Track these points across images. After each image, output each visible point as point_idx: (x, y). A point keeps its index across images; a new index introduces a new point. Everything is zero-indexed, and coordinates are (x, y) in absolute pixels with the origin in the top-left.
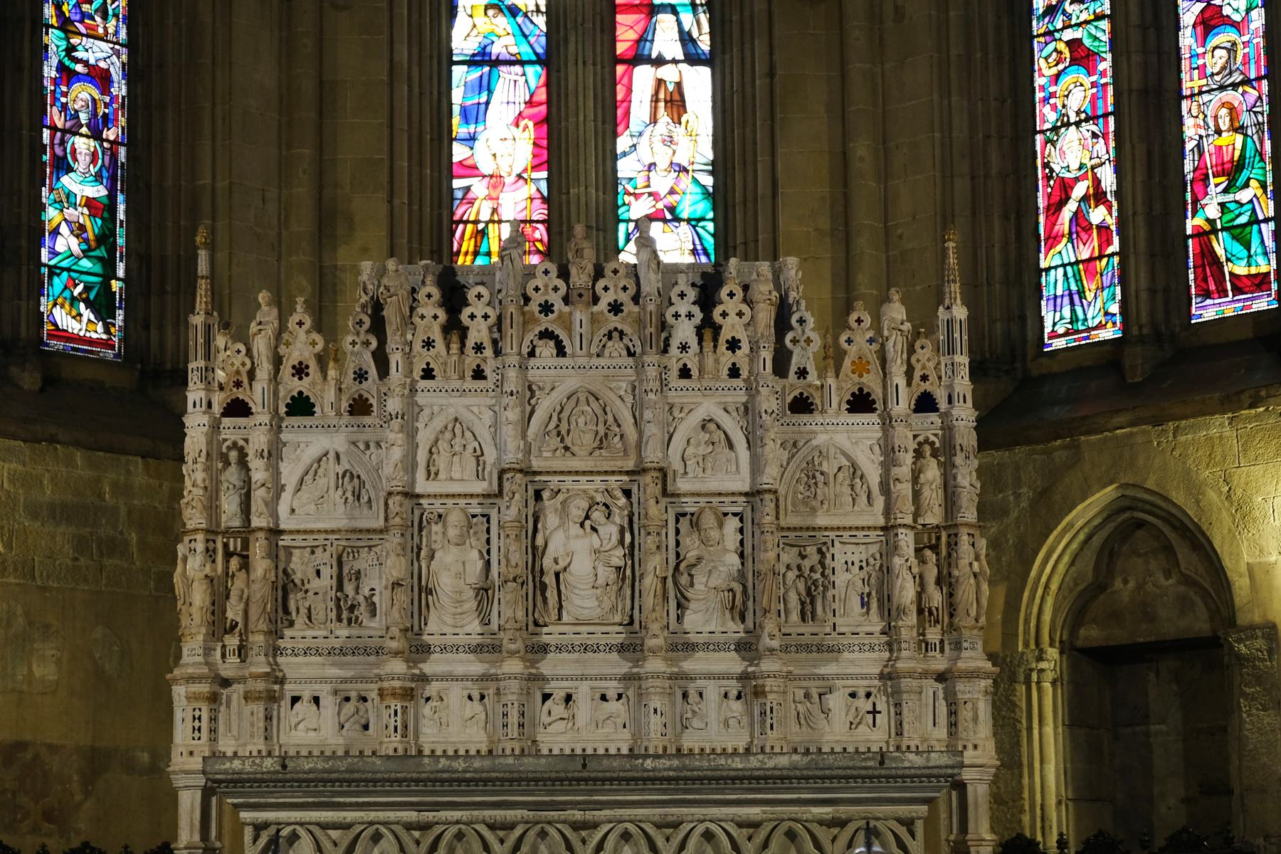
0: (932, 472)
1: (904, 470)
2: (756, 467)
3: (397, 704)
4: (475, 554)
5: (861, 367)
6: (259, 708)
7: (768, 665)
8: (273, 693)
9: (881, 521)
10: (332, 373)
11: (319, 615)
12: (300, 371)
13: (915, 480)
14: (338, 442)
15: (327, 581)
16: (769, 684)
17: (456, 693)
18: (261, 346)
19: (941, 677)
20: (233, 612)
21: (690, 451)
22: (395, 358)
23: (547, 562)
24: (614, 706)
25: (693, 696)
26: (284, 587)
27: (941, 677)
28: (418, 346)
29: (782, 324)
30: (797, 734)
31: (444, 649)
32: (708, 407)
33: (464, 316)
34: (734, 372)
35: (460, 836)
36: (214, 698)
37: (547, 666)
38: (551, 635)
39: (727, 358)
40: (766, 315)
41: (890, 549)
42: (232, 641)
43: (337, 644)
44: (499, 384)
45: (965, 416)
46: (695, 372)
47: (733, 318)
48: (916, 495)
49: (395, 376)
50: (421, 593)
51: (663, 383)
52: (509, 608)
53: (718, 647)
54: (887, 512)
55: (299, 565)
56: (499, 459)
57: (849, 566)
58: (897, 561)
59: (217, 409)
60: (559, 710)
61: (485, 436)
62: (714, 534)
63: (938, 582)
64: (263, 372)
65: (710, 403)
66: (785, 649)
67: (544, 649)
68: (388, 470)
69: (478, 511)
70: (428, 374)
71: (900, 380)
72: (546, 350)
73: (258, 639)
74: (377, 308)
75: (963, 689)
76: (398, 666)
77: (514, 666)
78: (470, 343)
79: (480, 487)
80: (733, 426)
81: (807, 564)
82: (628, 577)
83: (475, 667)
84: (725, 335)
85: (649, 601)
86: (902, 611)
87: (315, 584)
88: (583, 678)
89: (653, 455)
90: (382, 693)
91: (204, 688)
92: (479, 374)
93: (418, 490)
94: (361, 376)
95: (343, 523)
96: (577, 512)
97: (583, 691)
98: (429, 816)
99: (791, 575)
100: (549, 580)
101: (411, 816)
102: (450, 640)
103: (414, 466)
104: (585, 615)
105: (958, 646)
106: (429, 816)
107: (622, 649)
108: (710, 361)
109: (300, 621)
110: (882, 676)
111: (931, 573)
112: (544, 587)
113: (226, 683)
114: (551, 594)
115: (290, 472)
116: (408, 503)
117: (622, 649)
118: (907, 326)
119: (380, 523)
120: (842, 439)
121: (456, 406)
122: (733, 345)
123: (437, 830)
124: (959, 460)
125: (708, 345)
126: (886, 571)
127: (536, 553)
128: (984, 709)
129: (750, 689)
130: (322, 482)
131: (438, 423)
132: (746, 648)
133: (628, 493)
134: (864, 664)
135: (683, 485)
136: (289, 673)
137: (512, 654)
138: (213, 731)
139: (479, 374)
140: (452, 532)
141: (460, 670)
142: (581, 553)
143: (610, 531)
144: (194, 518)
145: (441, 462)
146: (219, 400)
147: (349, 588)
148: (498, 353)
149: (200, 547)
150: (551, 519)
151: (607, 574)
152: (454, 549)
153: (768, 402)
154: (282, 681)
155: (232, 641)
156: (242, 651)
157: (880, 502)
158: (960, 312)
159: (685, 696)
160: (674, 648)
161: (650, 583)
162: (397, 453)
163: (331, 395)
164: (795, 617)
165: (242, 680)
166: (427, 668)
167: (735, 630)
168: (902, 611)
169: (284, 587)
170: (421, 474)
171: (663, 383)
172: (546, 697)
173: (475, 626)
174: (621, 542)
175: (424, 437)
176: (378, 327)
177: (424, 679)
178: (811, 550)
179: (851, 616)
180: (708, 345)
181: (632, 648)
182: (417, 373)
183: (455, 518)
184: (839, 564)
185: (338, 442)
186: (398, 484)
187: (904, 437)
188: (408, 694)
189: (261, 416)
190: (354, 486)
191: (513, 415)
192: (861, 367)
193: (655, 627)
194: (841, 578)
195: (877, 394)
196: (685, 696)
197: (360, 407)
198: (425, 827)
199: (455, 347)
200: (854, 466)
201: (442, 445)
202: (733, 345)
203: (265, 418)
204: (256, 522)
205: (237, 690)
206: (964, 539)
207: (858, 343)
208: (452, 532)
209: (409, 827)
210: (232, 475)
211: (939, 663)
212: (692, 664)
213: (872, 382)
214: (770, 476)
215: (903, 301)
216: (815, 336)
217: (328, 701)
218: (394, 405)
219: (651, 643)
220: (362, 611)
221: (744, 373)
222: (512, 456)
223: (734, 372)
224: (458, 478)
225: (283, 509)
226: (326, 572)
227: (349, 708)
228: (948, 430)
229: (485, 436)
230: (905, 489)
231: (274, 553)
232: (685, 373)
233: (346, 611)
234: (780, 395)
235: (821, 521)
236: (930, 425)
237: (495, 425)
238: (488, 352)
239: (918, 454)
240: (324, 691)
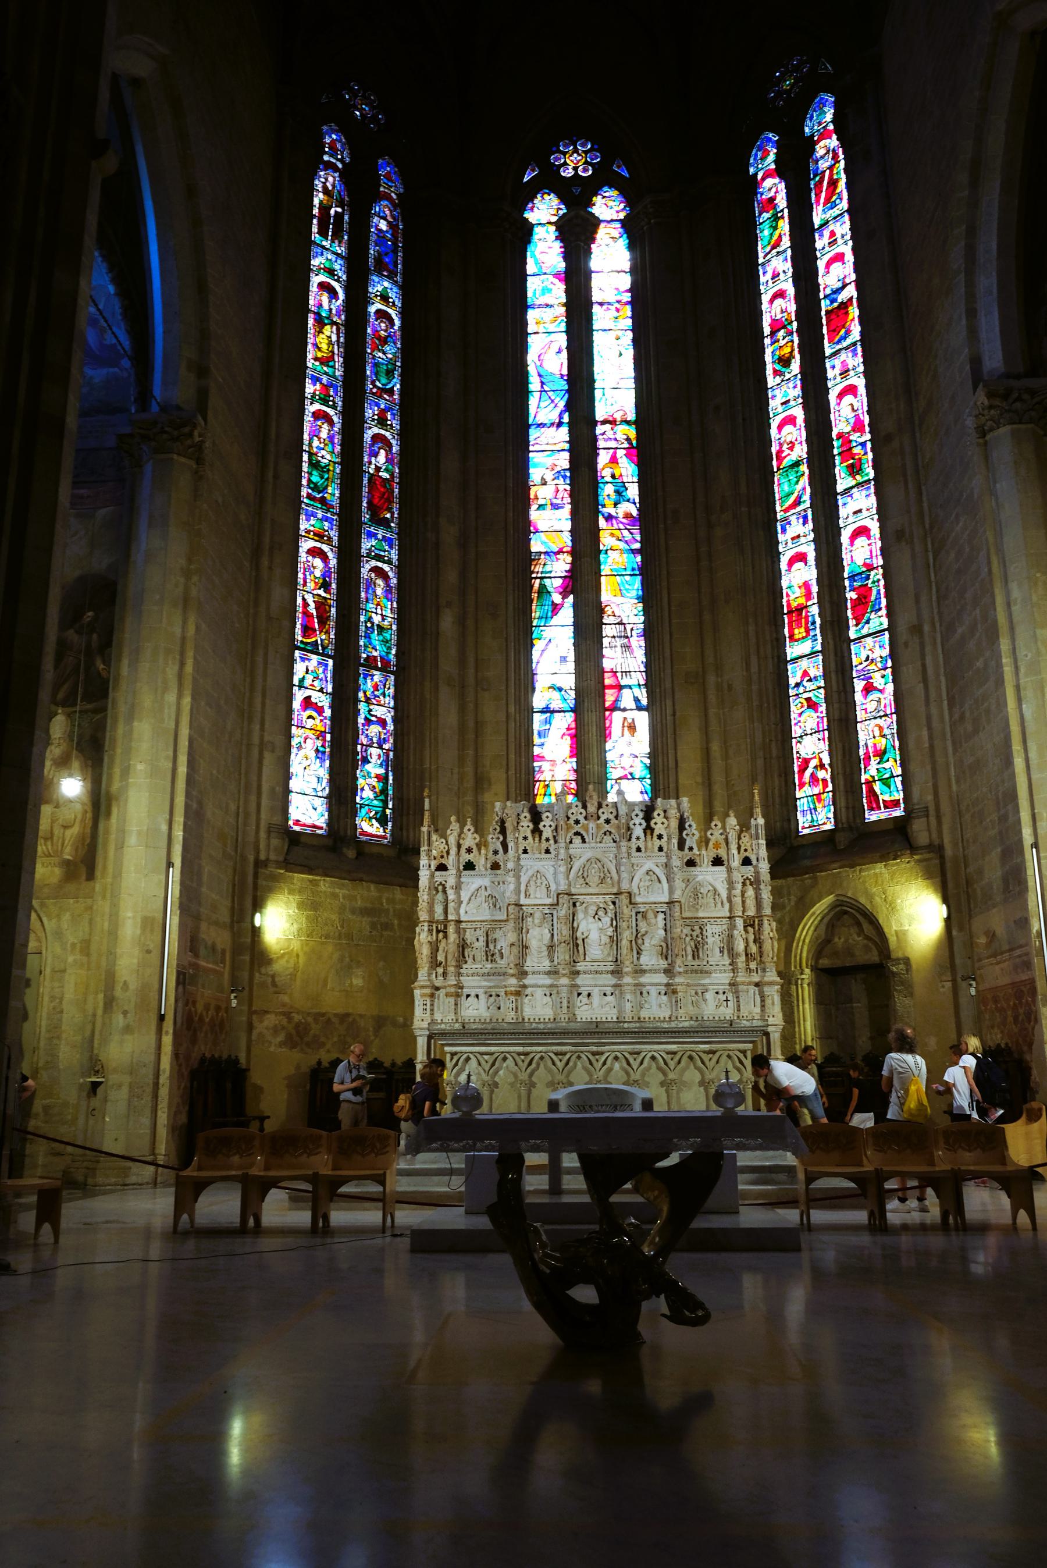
0: (750, 892)
1: (738, 892)
2: (671, 891)
3: (513, 998)
4: (547, 931)
5: (717, 846)
6: (452, 1000)
7: (678, 980)
8: (458, 994)
9: (728, 915)
10: (483, 851)
11: (478, 958)
12: (469, 851)
13: (743, 895)
14: (486, 882)
15: (481, 943)
16: (679, 988)
17: (539, 993)
18: (452, 840)
19: (757, 985)
20: (440, 957)
21: (642, 884)
22: (511, 845)
23: (579, 934)
24: (609, 998)
25: (645, 994)
26: (463, 946)
27: (757, 985)
28: (521, 839)
29: (681, 827)
30: (692, 1011)
31: (533, 973)
32: (649, 865)
33: (541, 826)
34: (661, 849)
35: (542, 1058)
36: (432, 996)
37: (579, 981)
38: (581, 966)
39: (657, 843)
40: (674, 824)
41: (732, 927)
42: (440, 970)
43: (486, 971)
44: (557, 856)
45: (764, 867)
46: (643, 849)
47: (659, 825)
48: (743, 902)
49: (511, 852)
50: (524, 947)
51: (629, 854)
52: (562, 954)
53: (656, 972)
54: (731, 910)
55: (469, 936)
56: (557, 889)
57: (714, 936)
58: (736, 932)
59: (433, 868)
60: (585, 1000)
61: (551, 878)
62: (653, 921)
63: (755, 941)
64: (453, 851)
65: (651, 863)
66: (686, 972)
67: (578, 973)
68: (508, 894)
69: (548, 911)
70: (525, 851)
71: (735, 852)
72: (577, 840)
73: (451, 969)
74: (502, 822)
75: (767, 990)
76: (513, 981)
77: (565, 981)
78: (544, 837)
79: (549, 901)
80: (660, 872)
81: (694, 934)
82: (615, 940)
83: (548, 981)
84: (656, 833)
85: (624, 951)
86: (738, 955)
87: (476, 944)
88: (596, 986)
89: (625, 886)
90: (506, 993)
91: (428, 991)
92: (547, 851)
93: (522, 903)
94: (496, 852)
95: (488, 918)
96: (592, 912)
97: (596, 992)
98: (528, 1049)
99: (688, 939)
100: (580, 942)
101: (520, 1049)
102: (536, 969)
103: (520, 892)
104: (597, 957)
105: (764, 970)
106: (528, 1049)
107: (613, 972)
108: (650, 844)
109: (470, 961)
110: (730, 984)
111: (751, 937)
112: (577, 945)
113: (437, 989)
114: (581, 948)
115: (465, 895)
116: (517, 908)
117: (613, 972)
118: (738, 827)
119: (505, 917)
120: (709, 878)
121: (538, 865)
122: (660, 837)
123: (532, 1055)
124: (762, 886)
125: (649, 837)
126: (731, 937)
127: (574, 930)
128: (777, 999)
129: (670, 990)
130: (479, 899)
131: (530, 873)
132: (668, 972)
133: (614, 903)
134: (721, 978)
135: (638, 899)
136: (465, 984)
137: (564, 975)
138: (432, 1010)
139: (547, 851)
140: (537, 921)
141: (541, 982)
142: (594, 931)
143: (607, 920)
144: (423, 916)
145: (531, 890)
146: (434, 864)
147: (491, 946)
148: (556, 842)
149: (426, 928)
150: (580, 915)
151: (605, 939)
152: (538, 929)
153: (676, 863)
154: (462, 988)
155: (440, 970)
156: (445, 974)
157: (727, 906)
158: (761, 821)
159: (641, 993)
160: (636, 972)
161: (625, 943)
162: (512, 887)
163: (482, 861)
164: (690, 957)
165: (445, 987)
166: (526, 982)
167: (663, 964)
168: (738, 955)
169: (463, 946)
170: (522, 895)
171: (629, 854)
172: (579, 994)
173: (547, 963)
174: (612, 925)
175: (524, 879)
176: (503, 831)
177: (525, 986)
178: (697, 928)
179: (715, 957)
180: (649, 837)
181: (617, 972)
182: (521, 851)
183: (538, 915)
184: (709, 934)
185: (486, 882)
186: (512, 900)
187: (737, 877)
188: (518, 994)
189: (452, 871)
190: (493, 901)
191: (563, 869)
192: (717, 846)
193: (627, 963)
194: (710, 940)
195: (725, 858)
196: (641, 993)
197: (495, 866)
198: (526, 1054)
199: (537, 839)
200: (715, 890)
201: (532, 883)
202: (660, 837)
203: (454, 872)
204: (450, 917)
205: (442, 992)
206: (766, 922)
207: (715, 835)
208: (537, 921)
209: (519, 1054)
210: (440, 896)
211: (756, 978)
212: (645, 979)
213: (722, 852)
214: (677, 895)
215: (735, 817)
216: (696, 832)
217: (482, 997)
218: (510, 865)
219: (626, 970)
220: (497, 957)
221: (665, 849)
222: (563, 887)
223: (661, 849)
224: (538, 898)
225: (462, 911)
226: (481, 939)
227: (492, 999)
228: (757, 873)
229: (551, 878)
230: (738, 900)
231: (458, 931)
232: (639, 850)
233: (490, 956)
234: (681, 858)
235: (701, 915)
236: (749, 871)
237: (555, 873)
238: (552, 842)
239: (744, 884)
240: (481, 992)
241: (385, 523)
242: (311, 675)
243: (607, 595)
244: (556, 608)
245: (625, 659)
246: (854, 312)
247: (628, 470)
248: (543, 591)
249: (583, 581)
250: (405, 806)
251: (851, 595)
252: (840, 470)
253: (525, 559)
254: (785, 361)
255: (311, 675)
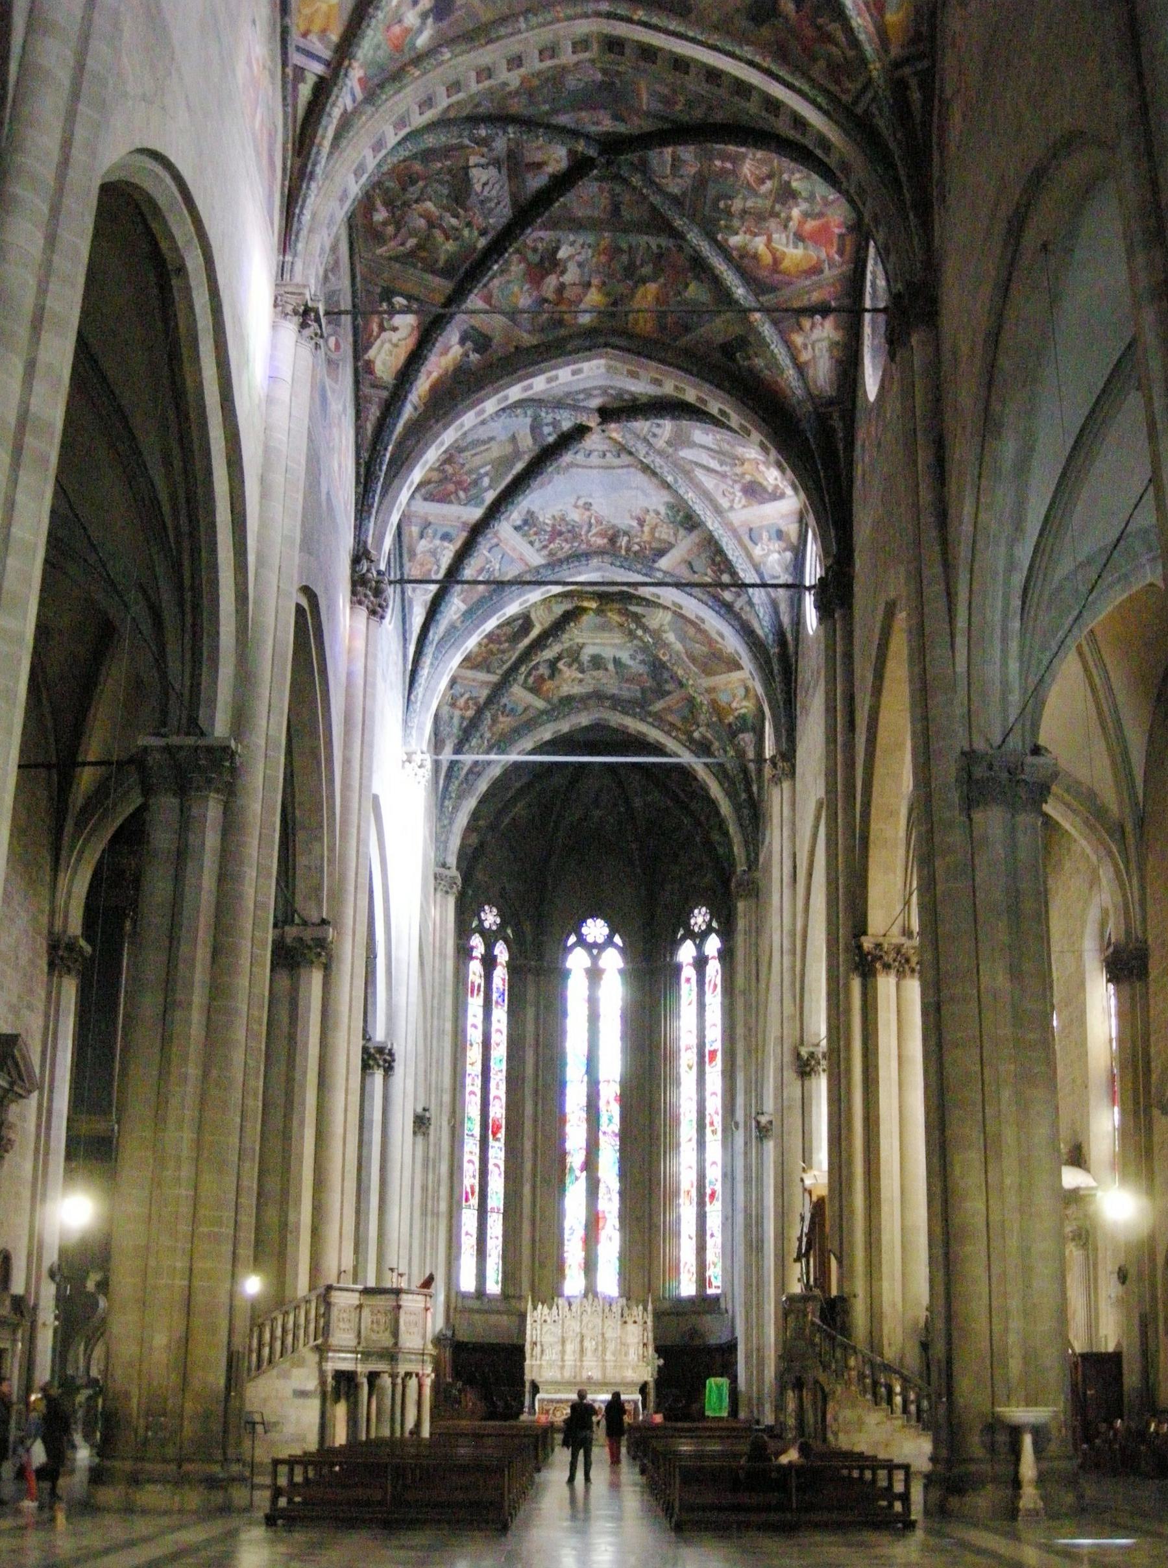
241: (498, 1140)
242: (469, 1219)
243: (602, 1173)
244: (577, 1178)
245: (610, 1204)
246: (719, 1054)
247: (615, 1109)
248: (571, 1169)
249: (590, 1165)
250: (509, 1276)
251: (708, 1191)
252: (708, 1130)
253: (563, 1154)
254: (690, 1068)
255: (469, 1219)
